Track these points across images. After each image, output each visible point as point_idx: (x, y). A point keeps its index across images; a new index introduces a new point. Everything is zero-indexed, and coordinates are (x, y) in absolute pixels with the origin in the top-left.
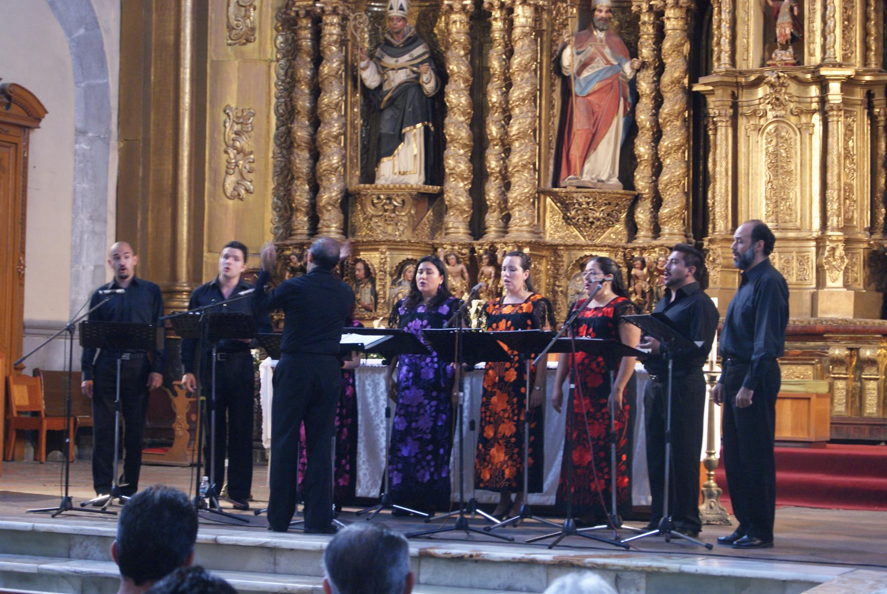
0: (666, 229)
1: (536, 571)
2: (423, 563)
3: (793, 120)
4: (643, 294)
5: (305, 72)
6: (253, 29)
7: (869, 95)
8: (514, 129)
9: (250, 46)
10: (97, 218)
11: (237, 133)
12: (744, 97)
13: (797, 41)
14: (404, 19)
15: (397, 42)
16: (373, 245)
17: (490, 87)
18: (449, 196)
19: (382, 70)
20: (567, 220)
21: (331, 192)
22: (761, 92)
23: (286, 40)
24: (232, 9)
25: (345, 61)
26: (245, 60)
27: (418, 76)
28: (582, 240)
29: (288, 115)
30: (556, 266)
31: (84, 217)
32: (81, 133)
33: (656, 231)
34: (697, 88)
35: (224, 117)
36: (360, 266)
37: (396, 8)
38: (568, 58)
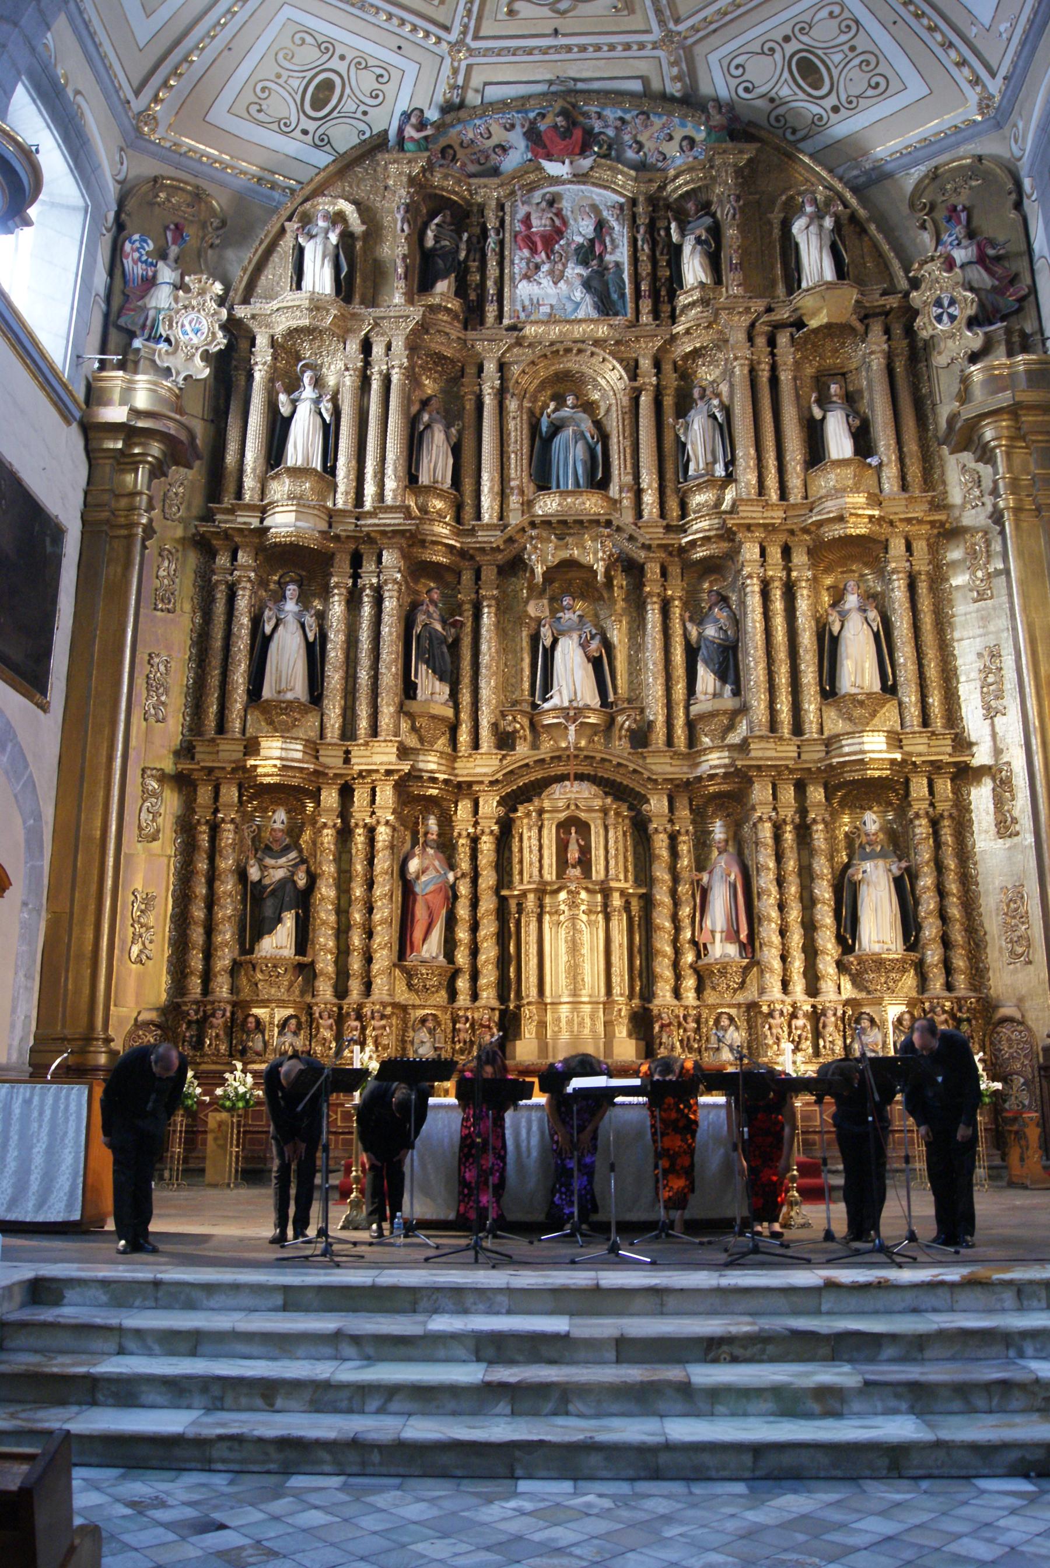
0: (484, 994)
1: (940, 1291)
2: (824, 1293)
3: (584, 917)
4: (465, 1042)
5: (202, 866)
6: (158, 831)
7: (628, 903)
8: (377, 917)
9: (156, 845)
10: (29, 977)
11: (142, 911)
12: (547, 900)
13: (585, 863)
14: (282, 830)
15: (276, 847)
16: (264, 1003)
17: (353, 885)
18: (319, 966)
19: (263, 868)
20: (410, 986)
21: (224, 960)
22: (563, 895)
23: (183, 842)
24: (144, 815)
25: (238, 862)
26: (151, 855)
27: (293, 874)
28: (418, 1002)
29: (183, 899)
30: (405, 1021)
31: (21, 974)
32: (25, 904)
33: (475, 996)
34: (504, 893)
35: (132, 898)
36: (251, 1019)
37: (279, 822)
38: (414, 865)
